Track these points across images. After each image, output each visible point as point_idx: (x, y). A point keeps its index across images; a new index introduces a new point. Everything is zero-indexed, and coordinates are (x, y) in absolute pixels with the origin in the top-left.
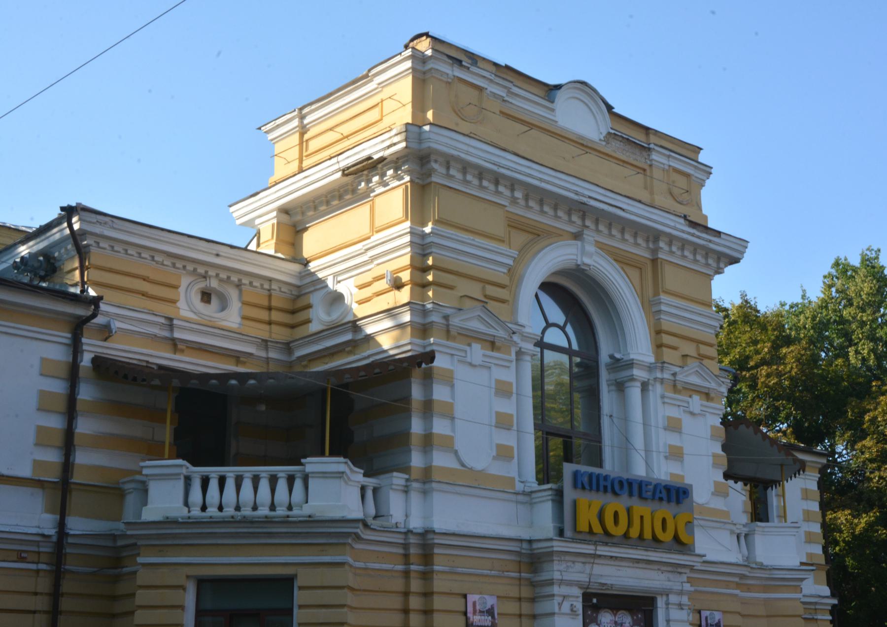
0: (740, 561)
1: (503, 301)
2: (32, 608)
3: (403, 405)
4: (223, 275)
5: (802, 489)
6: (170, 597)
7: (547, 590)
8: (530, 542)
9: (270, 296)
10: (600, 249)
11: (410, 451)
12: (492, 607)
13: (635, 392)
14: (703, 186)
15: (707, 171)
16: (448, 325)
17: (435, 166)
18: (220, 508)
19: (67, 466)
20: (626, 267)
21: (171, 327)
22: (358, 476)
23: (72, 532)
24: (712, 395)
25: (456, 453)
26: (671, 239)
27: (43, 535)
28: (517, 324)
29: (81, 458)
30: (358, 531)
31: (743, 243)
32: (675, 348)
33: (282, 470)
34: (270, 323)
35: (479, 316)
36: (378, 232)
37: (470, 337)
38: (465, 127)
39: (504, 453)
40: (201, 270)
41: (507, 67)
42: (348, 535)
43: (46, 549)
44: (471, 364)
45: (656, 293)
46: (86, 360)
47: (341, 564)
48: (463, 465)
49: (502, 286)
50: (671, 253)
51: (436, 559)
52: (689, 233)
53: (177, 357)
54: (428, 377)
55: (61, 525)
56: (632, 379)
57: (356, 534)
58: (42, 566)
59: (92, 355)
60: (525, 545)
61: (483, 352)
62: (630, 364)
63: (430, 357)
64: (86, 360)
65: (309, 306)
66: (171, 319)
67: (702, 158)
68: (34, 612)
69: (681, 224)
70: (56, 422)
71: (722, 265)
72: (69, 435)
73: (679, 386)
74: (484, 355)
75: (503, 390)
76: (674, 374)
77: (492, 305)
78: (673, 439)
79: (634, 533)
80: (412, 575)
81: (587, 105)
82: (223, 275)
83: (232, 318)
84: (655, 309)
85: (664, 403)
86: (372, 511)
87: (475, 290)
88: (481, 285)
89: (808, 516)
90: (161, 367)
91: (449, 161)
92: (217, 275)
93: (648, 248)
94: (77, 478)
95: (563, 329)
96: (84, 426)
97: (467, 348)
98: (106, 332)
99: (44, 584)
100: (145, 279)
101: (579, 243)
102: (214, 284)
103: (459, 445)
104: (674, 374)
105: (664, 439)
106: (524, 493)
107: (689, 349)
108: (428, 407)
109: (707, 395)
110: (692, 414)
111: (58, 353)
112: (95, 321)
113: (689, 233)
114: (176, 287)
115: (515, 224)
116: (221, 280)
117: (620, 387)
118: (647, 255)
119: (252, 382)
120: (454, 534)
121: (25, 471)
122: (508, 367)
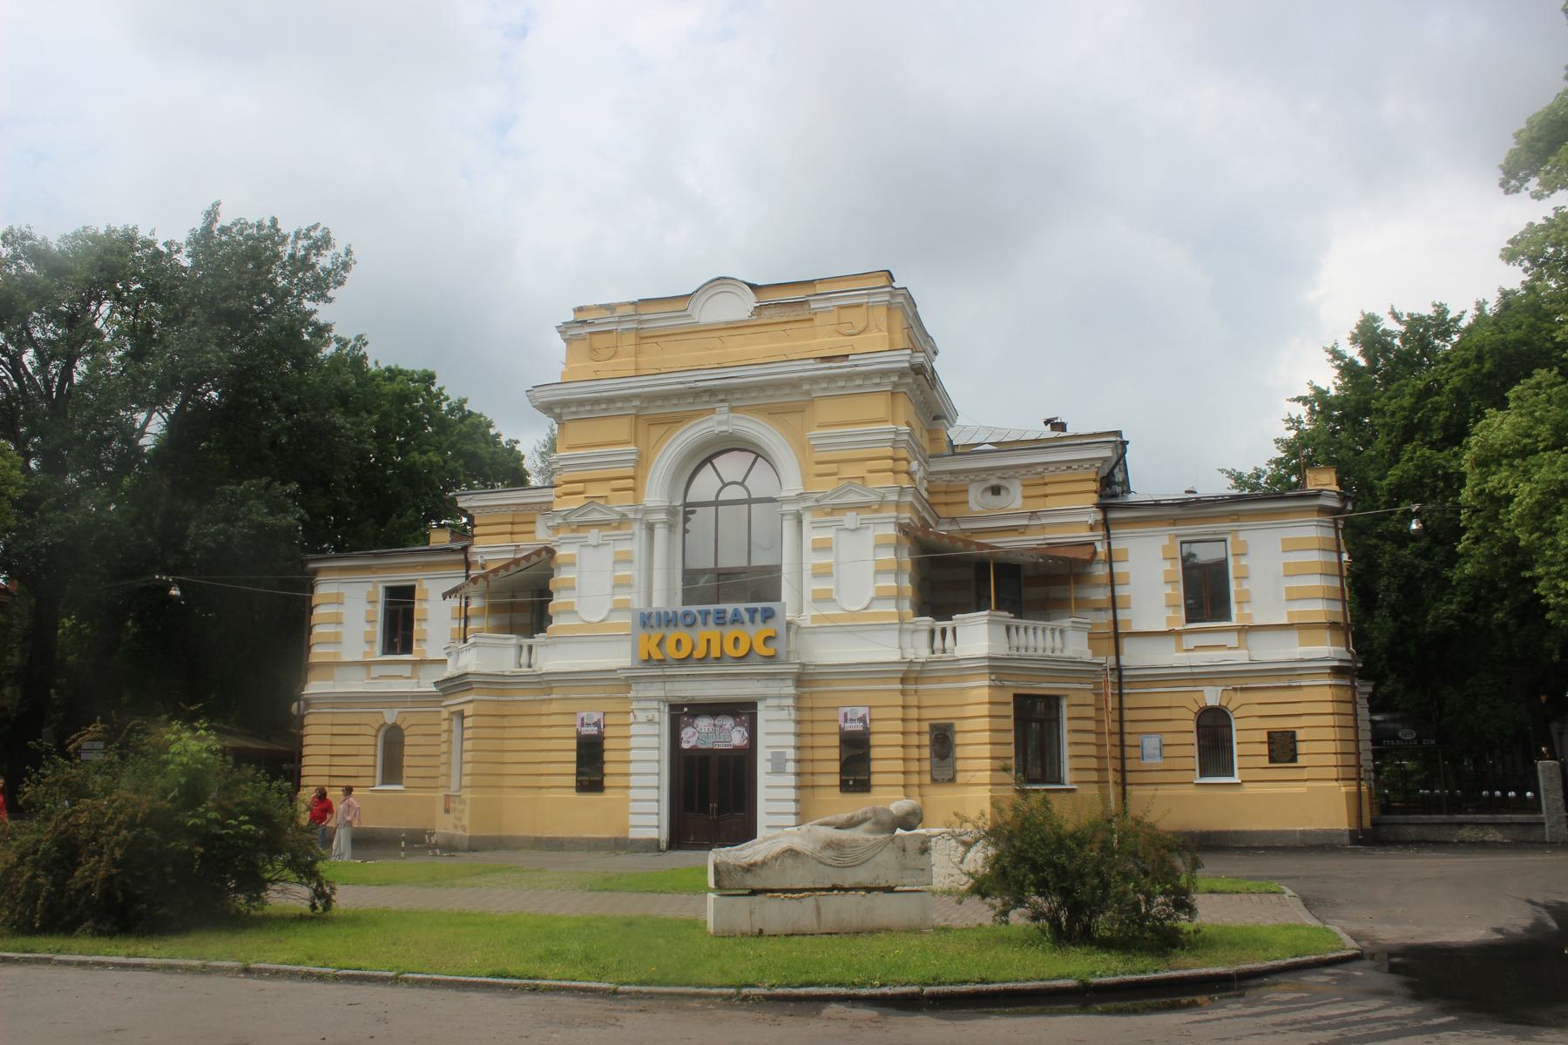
12: (599, 720)
26: (814, 380)
48: (585, 621)
52: (825, 368)
69: (812, 364)
113: (825, 368)
122: (631, 539)
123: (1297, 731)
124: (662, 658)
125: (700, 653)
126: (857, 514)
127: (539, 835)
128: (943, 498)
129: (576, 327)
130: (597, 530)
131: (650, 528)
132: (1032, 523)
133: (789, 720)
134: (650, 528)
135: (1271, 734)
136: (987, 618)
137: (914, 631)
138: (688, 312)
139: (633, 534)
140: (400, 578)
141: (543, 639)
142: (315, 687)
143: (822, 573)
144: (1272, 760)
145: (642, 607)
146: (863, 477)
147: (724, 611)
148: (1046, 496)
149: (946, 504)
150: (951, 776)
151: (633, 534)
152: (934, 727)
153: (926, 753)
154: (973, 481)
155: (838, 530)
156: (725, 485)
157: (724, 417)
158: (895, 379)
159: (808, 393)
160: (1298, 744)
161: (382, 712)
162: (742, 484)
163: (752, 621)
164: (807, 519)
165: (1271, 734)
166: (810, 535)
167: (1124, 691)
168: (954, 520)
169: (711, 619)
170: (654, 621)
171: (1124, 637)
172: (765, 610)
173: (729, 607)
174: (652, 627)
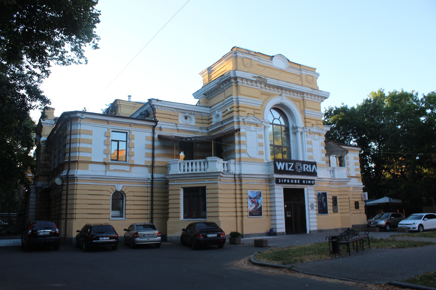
0: (330, 177)
1: (260, 114)
2: (147, 196)
3: (233, 142)
4: (190, 112)
5: (354, 157)
6: (176, 192)
7: (273, 188)
8: (268, 175)
9: (202, 116)
10: (288, 98)
11: (235, 154)
13: (299, 135)
14: (317, 79)
15: (318, 75)
16: (244, 121)
17: (238, 80)
18: (188, 171)
19: (153, 162)
20: (295, 102)
21: (177, 126)
22: (221, 161)
23: (155, 177)
24: (321, 134)
25: (248, 153)
26: (307, 94)
27: (148, 178)
28: (263, 119)
29: (156, 159)
30: (221, 175)
31: (329, 94)
32: (310, 123)
33: (202, 161)
34: (203, 123)
35: (253, 118)
36: (226, 98)
37: (250, 123)
38: (247, 70)
39: (261, 153)
40: (184, 111)
41: (258, 53)
42: (218, 176)
43: (149, 181)
44: (251, 131)
45: (304, 108)
46: (156, 136)
47: (217, 183)
48: (250, 157)
49: (260, 110)
50: (308, 97)
51: (243, 181)
53: (179, 133)
54: (239, 135)
55: (152, 176)
56: (298, 131)
57: (220, 176)
58: (149, 186)
59: (158, 135)
60: (267, 176)
61: (254, 127)
62: (297, 128)
63: (239, 130)
64: (156, 136)
65: (212, 118)
66: (177, 124)
67: (317, 71)
68: (148, 196)
70: (150, 151)
71: (323, 99)
72: (153, 154)
73: (311, 132)
74: (255, 128)
75: (260, 137)
76: (309, 129)
77: (256, 115)
78: (310, 146)
80: (237, 185)
82: (190, 112)
83: (193, 123)
84: (304, 112)
85: (307, 137)
86: (226, 169)
87: (251, 111)
88: (253, 110)
89: (356, 164)
90: (175, 136)
91: (242, 79)
92: (188, 112)
93: (301, 97)
94: (156, 164)
95: (279, 119)
96: (157, 152)
97: (250, 127)
98: (160, 129)
99: (149, 190)
100: (170, 115)
101: (281, 97)
102: (187, 114)
103: (248, 151)
104: (309, 129)
105: (307, 146)
106: (267, 163)
107: (314, 122)
108: (240, 142)
109: (320, 135)
110: (315, 140)
111: (150, 135)
112: (157, 126)
114: (178, 116)
115: (263, 94)
116: (189, 114)
117: (295, 133)
118: (301, 98)
119: (184, 140)
120: (247, 174)
121: (143, 163)
122: (262, 131)
129: (241, 53)
144: (356, 208)
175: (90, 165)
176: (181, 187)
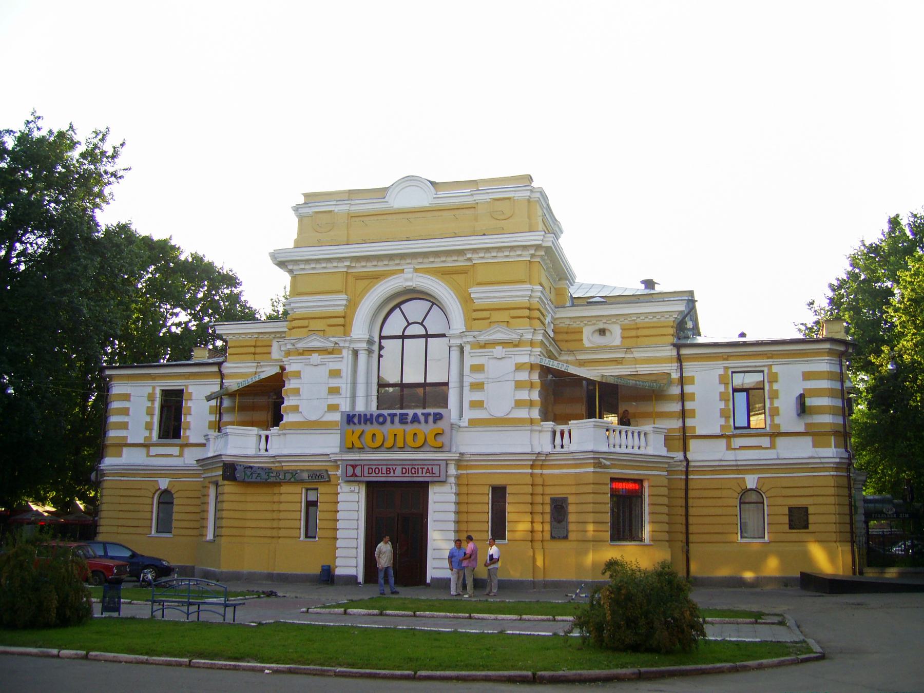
79: (400, 443)
81: (418, 186)
123: (809, 506)
124: (361, 446)
125: (389, 443)
126: (503, 348)
127: (270, 571)
128: (564, 337)
130: (317, 354)
131: (355, 353)
132: (628, 356)
133: (452, 493)
134: (355, 353)
135: (791, 509)
136: (594, 423)
137: (540, 431)
138: (386, 199)
139: (342, 358)
140: (173, 384)
141: (276, 431)
142: (109, 462)
143: (477, 386)
144: (791, 527)
145: (348, 410)
146: (508, 322)
147: (407, 414)
148: (638, 337)
149: (566, 341)
150: (565, 535)
151: (342, 358)
152: (554, 500)
153: (548, 518)
154: (586, 324)
155: (489, 358)
156: (409, 324)
157: (410, 276)
158: (532, 252)
159: (470, 259)
160: (810, 517)
161: (157, 481)
162: (421, 324)
163: (426, 422)
164: (467, 349)
165: (791, 509)
166: (469, 361)
167: (689, 477)
168: (571, 352)
169: (397, 419)
170: (356, 420)
171: (692, 438)
172: (435, 414)
173: (411, 412)
174: (355, 424)
175: (125, 450)
176: (209, 482)
